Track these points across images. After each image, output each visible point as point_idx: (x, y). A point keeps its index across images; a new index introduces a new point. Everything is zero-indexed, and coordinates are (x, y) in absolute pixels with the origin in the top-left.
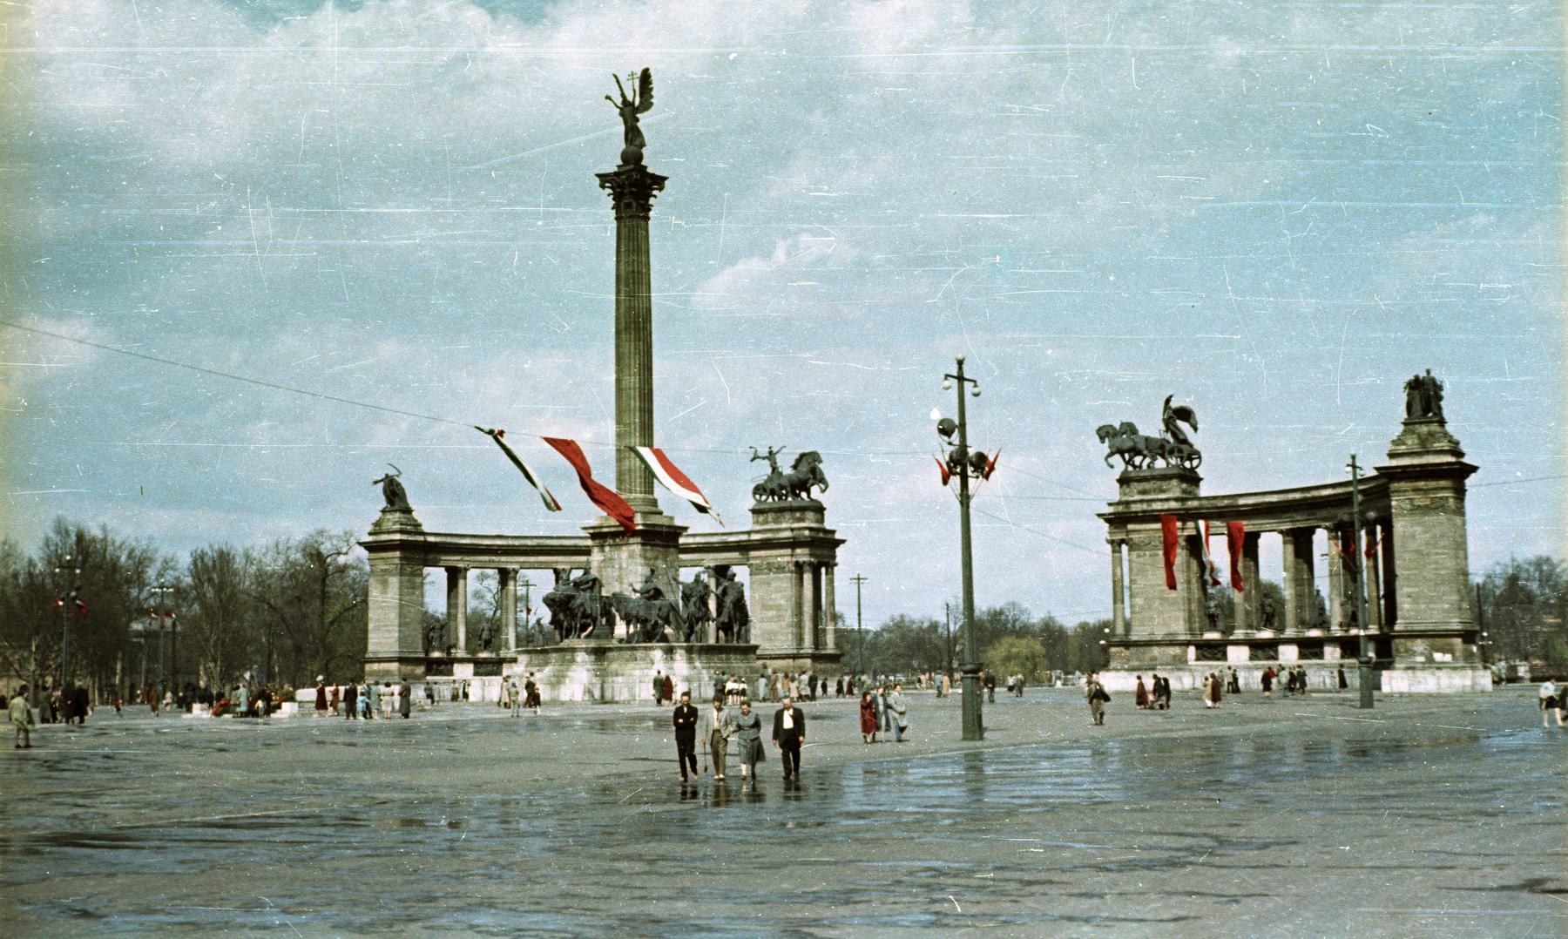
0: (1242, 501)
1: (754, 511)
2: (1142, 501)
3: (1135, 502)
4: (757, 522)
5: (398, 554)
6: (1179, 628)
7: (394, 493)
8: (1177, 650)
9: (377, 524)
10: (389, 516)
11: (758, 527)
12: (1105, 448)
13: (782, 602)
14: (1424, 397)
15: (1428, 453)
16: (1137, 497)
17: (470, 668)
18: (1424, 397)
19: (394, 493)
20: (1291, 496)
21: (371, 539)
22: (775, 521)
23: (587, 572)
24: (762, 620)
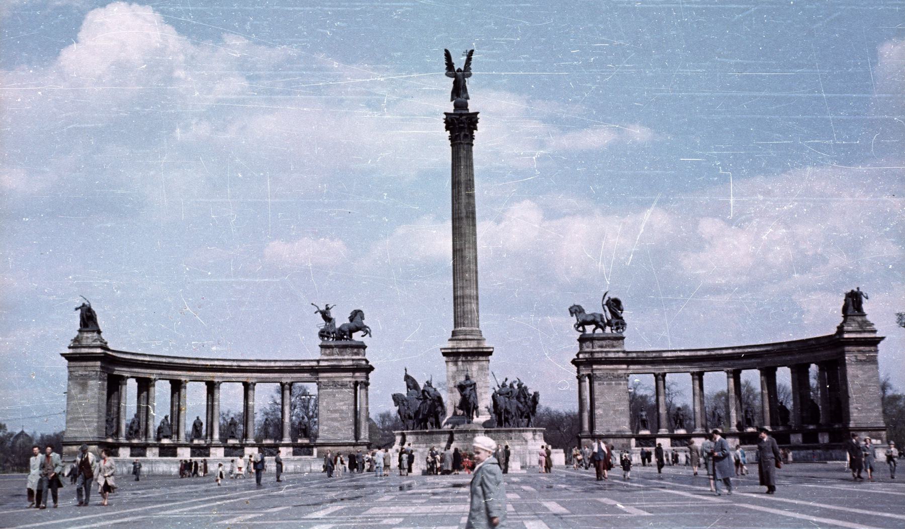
0: (665, 355)
1: (322, 346)
2: (602, 352)
3: (598, 352)
4: (325, 354)
5: (99, 363)
6: (626, 428)
7: (88, 319)
8: (625, 441)
9: (76, 340)
10: (85, 335)
11: (326, 358)
12: (574, 320)
13: (344, 408)
14: (854, 302)
15: (865, 332)
16: (598, 349)
17: (156, 450)
18: (854, 302)
19: (88, 319)
20: (699, 353)
21: (71, 351)
22: (341, 354)
23: (467, 378)
24: (328, 419)
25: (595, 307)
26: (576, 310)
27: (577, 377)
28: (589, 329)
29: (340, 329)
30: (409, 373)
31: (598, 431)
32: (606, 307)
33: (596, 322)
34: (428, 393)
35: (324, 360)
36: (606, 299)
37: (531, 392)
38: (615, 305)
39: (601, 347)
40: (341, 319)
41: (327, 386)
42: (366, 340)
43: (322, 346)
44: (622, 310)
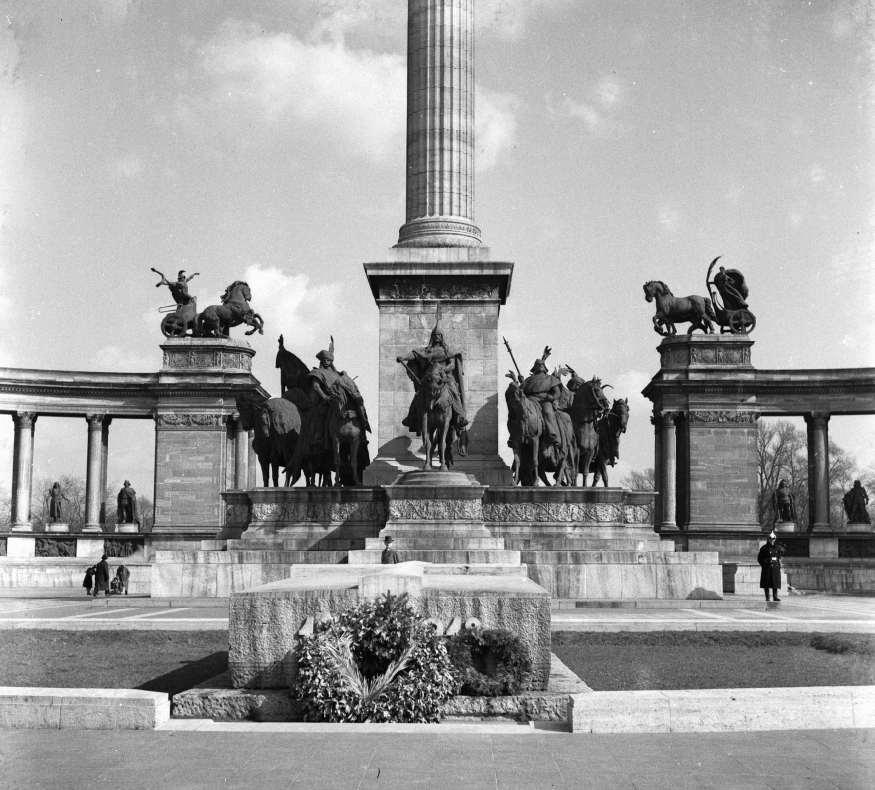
25: (690, 284)
26: (655, 291)
27: (654, 421)
28: (682, 328)
29: (202, 316)
30: (287, 347)
31: (698, 520)
32: (714, 288)
33: (693, 312)
34: (323, 386)
35: (167, 374)
36: (716, 271)
37: (611, 396)
38: (731, 284)
39: (705, 360)
40: (207, 298)
41: (173, 424)
42: (255, 341)
43: (164, 348)
44: (745, 295)
